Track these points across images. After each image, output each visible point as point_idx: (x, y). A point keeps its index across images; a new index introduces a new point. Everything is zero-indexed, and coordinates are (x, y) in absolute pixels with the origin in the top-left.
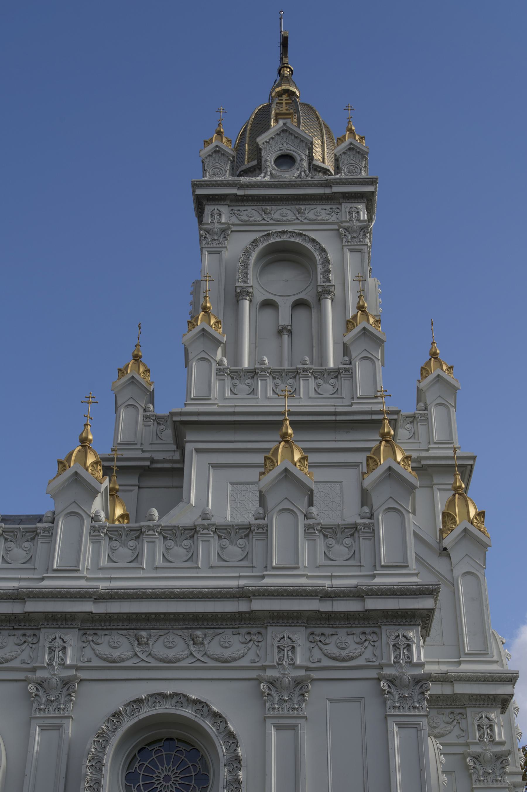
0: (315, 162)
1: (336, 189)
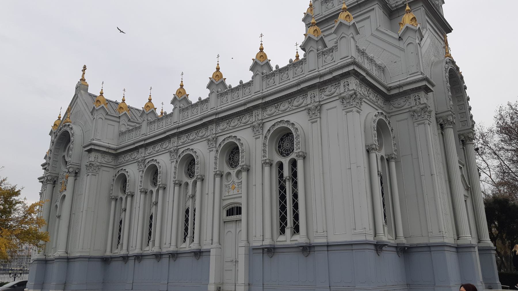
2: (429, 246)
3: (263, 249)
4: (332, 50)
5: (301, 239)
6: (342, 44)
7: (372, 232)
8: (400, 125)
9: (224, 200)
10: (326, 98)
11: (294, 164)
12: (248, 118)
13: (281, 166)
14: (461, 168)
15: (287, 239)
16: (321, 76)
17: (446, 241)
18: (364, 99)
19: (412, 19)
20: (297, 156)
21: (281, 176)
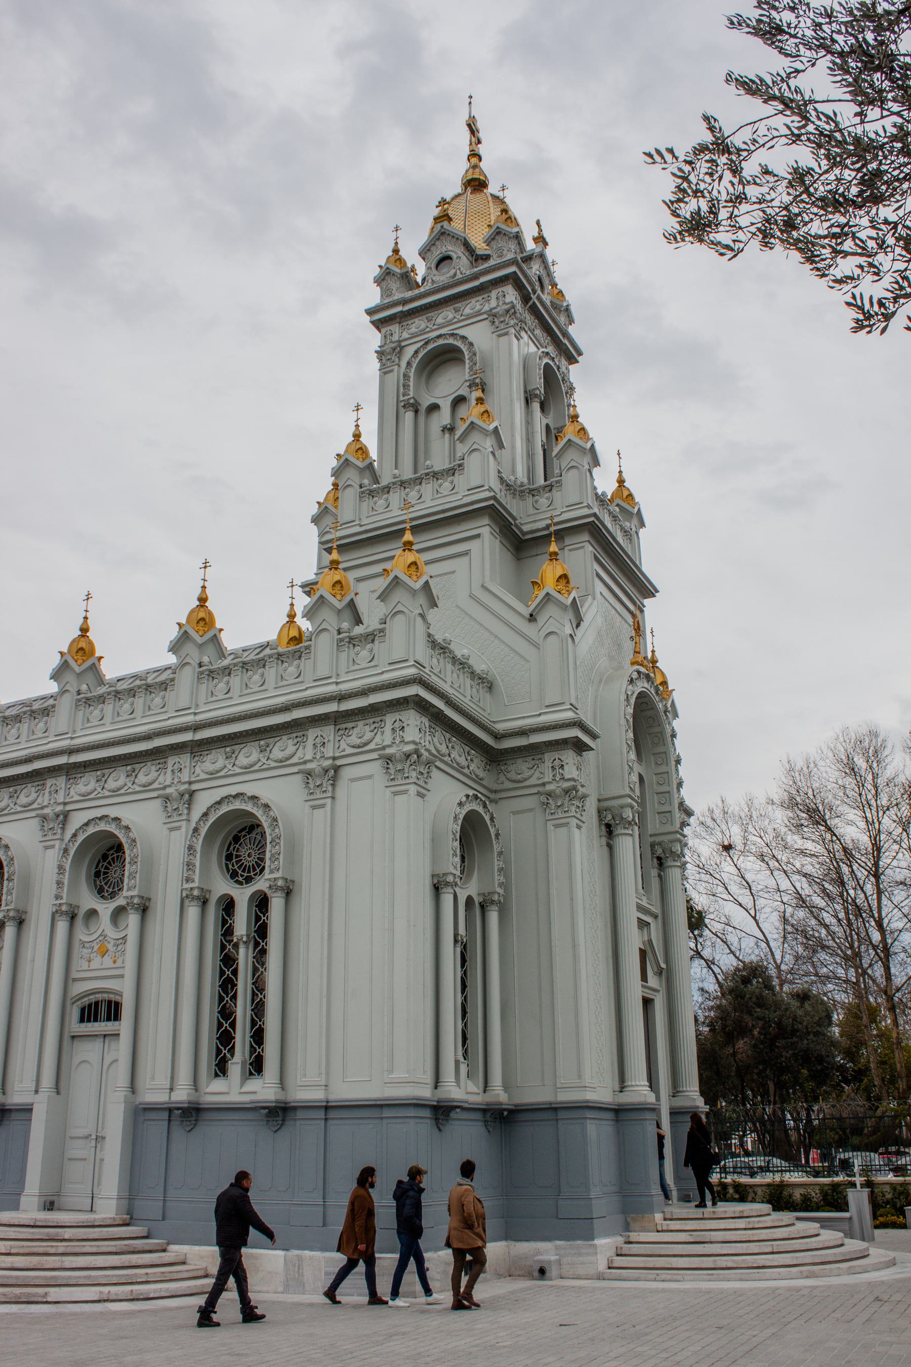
0: (479, 252)
1: (483, 279)
2: (556, 1109)
3: (170, 1110)
4: (371, 637)
5: (263, 1089)
6: (397, 627)
7: (429, 1078)
8: (514, 822)
9: (74, 980)
10: (350, 751)
11: (261, 903)
12: (154, 774)
13: (228, 905)
14: (642, 924)
15: (232, 1089)
16: (342, 697)
17: (591, 1096)
18: (438, 763)
19: (560, 577)
20: (270, 887)
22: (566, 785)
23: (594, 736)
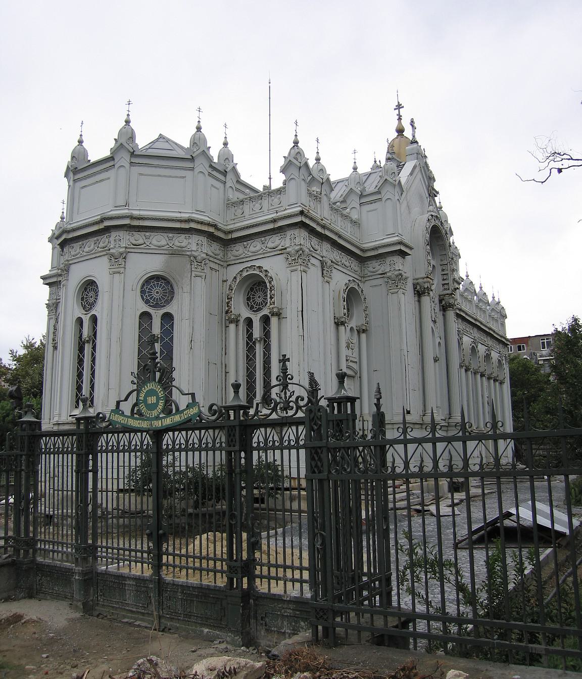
8: (372, 291)
21: (250, 336)
22: (397, 273)
23: (411, 248)
